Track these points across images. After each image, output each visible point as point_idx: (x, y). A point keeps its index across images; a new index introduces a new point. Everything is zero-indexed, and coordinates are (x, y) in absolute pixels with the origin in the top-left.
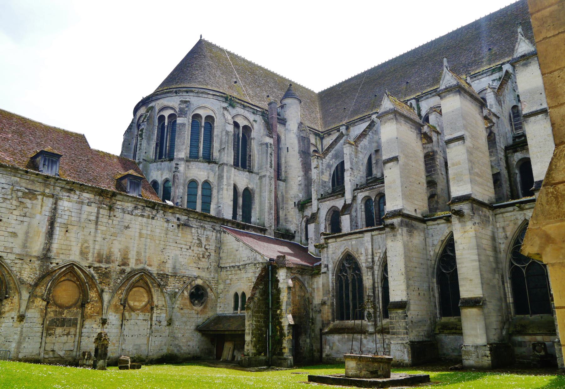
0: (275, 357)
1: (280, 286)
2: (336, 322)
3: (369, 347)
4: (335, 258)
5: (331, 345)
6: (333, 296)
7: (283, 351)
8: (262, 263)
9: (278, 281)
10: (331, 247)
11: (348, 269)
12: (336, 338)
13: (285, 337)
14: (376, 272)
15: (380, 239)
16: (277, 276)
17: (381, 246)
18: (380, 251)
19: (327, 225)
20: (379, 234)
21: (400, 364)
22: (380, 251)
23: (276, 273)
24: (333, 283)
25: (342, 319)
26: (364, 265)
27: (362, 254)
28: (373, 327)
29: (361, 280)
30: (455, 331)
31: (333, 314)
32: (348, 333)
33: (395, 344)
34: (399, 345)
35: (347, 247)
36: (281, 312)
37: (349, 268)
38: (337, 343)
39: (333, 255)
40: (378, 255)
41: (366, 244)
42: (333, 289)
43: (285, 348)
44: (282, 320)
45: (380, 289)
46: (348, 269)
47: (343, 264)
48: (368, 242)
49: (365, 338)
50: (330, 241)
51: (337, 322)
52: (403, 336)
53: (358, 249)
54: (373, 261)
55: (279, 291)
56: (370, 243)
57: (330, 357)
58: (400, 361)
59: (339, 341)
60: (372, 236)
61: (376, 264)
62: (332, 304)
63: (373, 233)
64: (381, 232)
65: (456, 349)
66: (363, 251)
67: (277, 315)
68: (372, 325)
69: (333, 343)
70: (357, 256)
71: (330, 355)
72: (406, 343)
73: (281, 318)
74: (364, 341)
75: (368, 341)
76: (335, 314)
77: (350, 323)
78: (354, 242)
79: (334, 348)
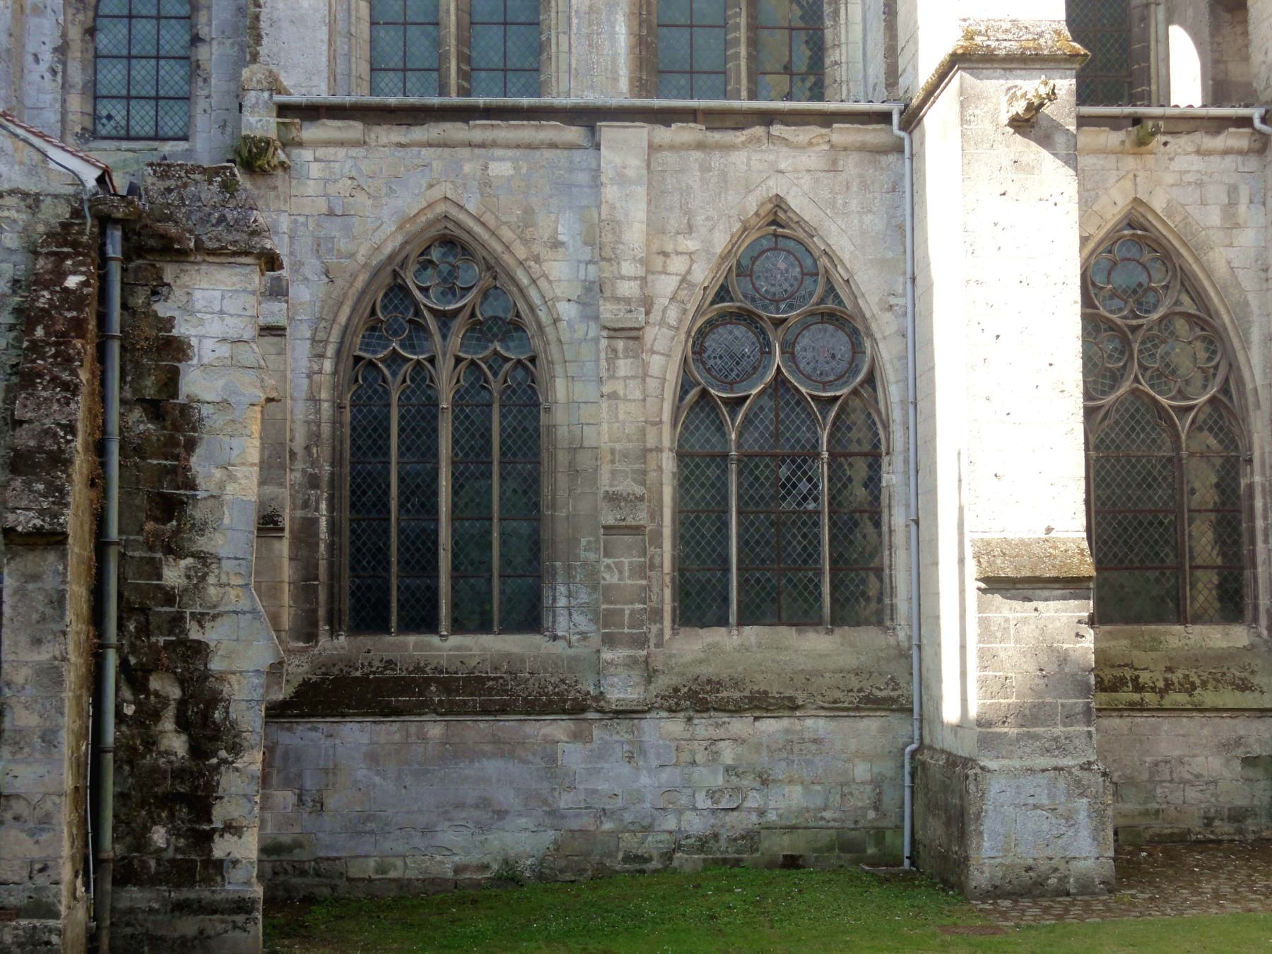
0: (135, 896)
1: (196, 383)
2: (324, 641)
3: (603, 786)
4: (343, 244)
5: (309, 783)
6: (313, 482)
7: (221, 848)
8: (32, 201)
9: (174, 349)
10: (315, 170)
11: (432, 324)
12: (355, 736)
13: (236, 749)
14: (656, 363)
15: (693, 179)
16: (162, 309)
17: (699, 220)
18: (691, 244)
19: (75, 33)
20: (700, 146)
21: (1040, 883)
22: (691, 244)
23: (158, 289)
24: (314, 400)
25: (368, 616)
26: (567, 311)
27: (556, 245)
28: (636, 676)
29: (527, 397)
30: (1136, 697)
31: (305, 588)
32: (451, 709)
33: (1011, 773)
34: (1042, 779)
35: (446, 189)
36: (198, 580)
37: (445, 318)
38: (362, 773)
39: (333, 228)
40: (678, 265)
41: (610, 192)
42: (314, 438)
43: (232, 828)
44: (212, 635)
45: (668, 463)
46: (432, 324)
47: (397, 291)
48: (621, 179)
49: (576, 737)
50: (310, 132)
51: (336, 646)
52: (1059, 730)
53: (529, 211)
54: (647, 303)
55: (173, 423)
56: (641, 191)
57: (298, 855)
58: (1044, 867)
59: (373, 758)
60: (653, 148)
61: (656, 316)
62: (306, 531)
63: (663, 134)
64: (717, 136)
65: (1131, 781)
66: (567, 228)
67: (169, 597)
68: (632, 663)
69: (330, 771)
70: (521, 252)
71: (298, 845)
72: (1086, 767)
73: (200, 619)
74: (573, 756)
75: (601, 754)
76: (322, 596)
77: (448, 648)
78: (501, 168)
79: (331, 802)
